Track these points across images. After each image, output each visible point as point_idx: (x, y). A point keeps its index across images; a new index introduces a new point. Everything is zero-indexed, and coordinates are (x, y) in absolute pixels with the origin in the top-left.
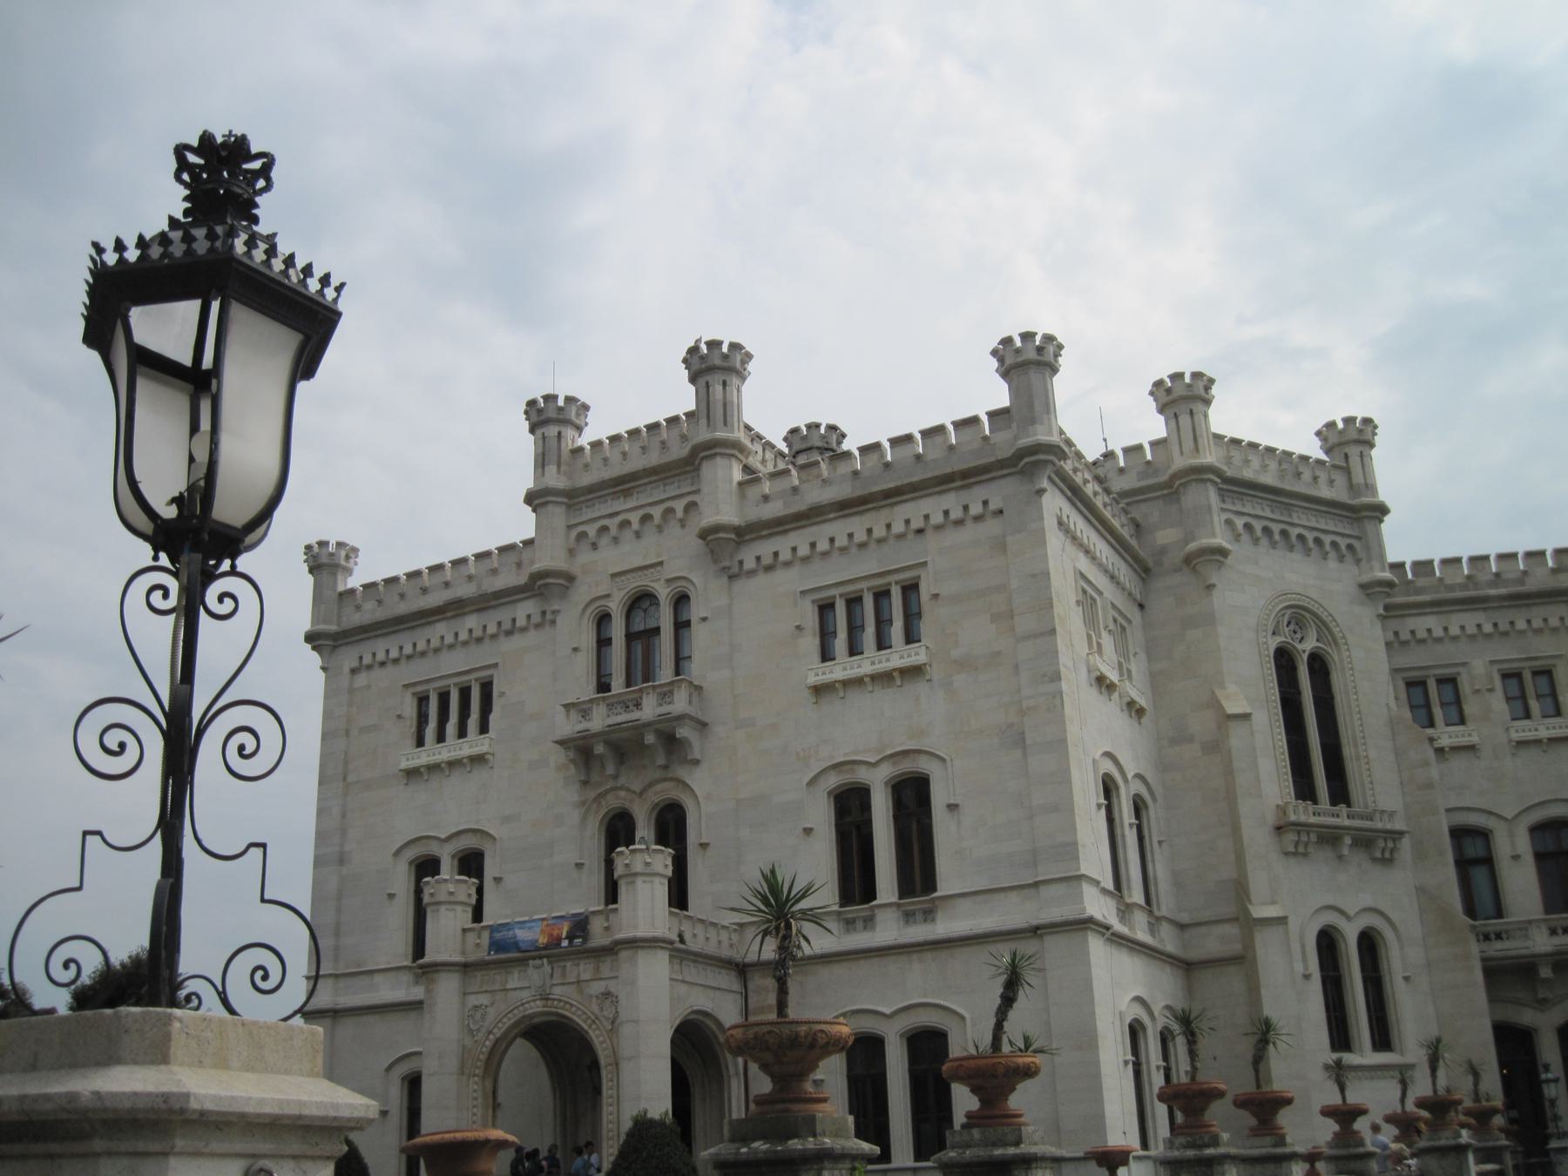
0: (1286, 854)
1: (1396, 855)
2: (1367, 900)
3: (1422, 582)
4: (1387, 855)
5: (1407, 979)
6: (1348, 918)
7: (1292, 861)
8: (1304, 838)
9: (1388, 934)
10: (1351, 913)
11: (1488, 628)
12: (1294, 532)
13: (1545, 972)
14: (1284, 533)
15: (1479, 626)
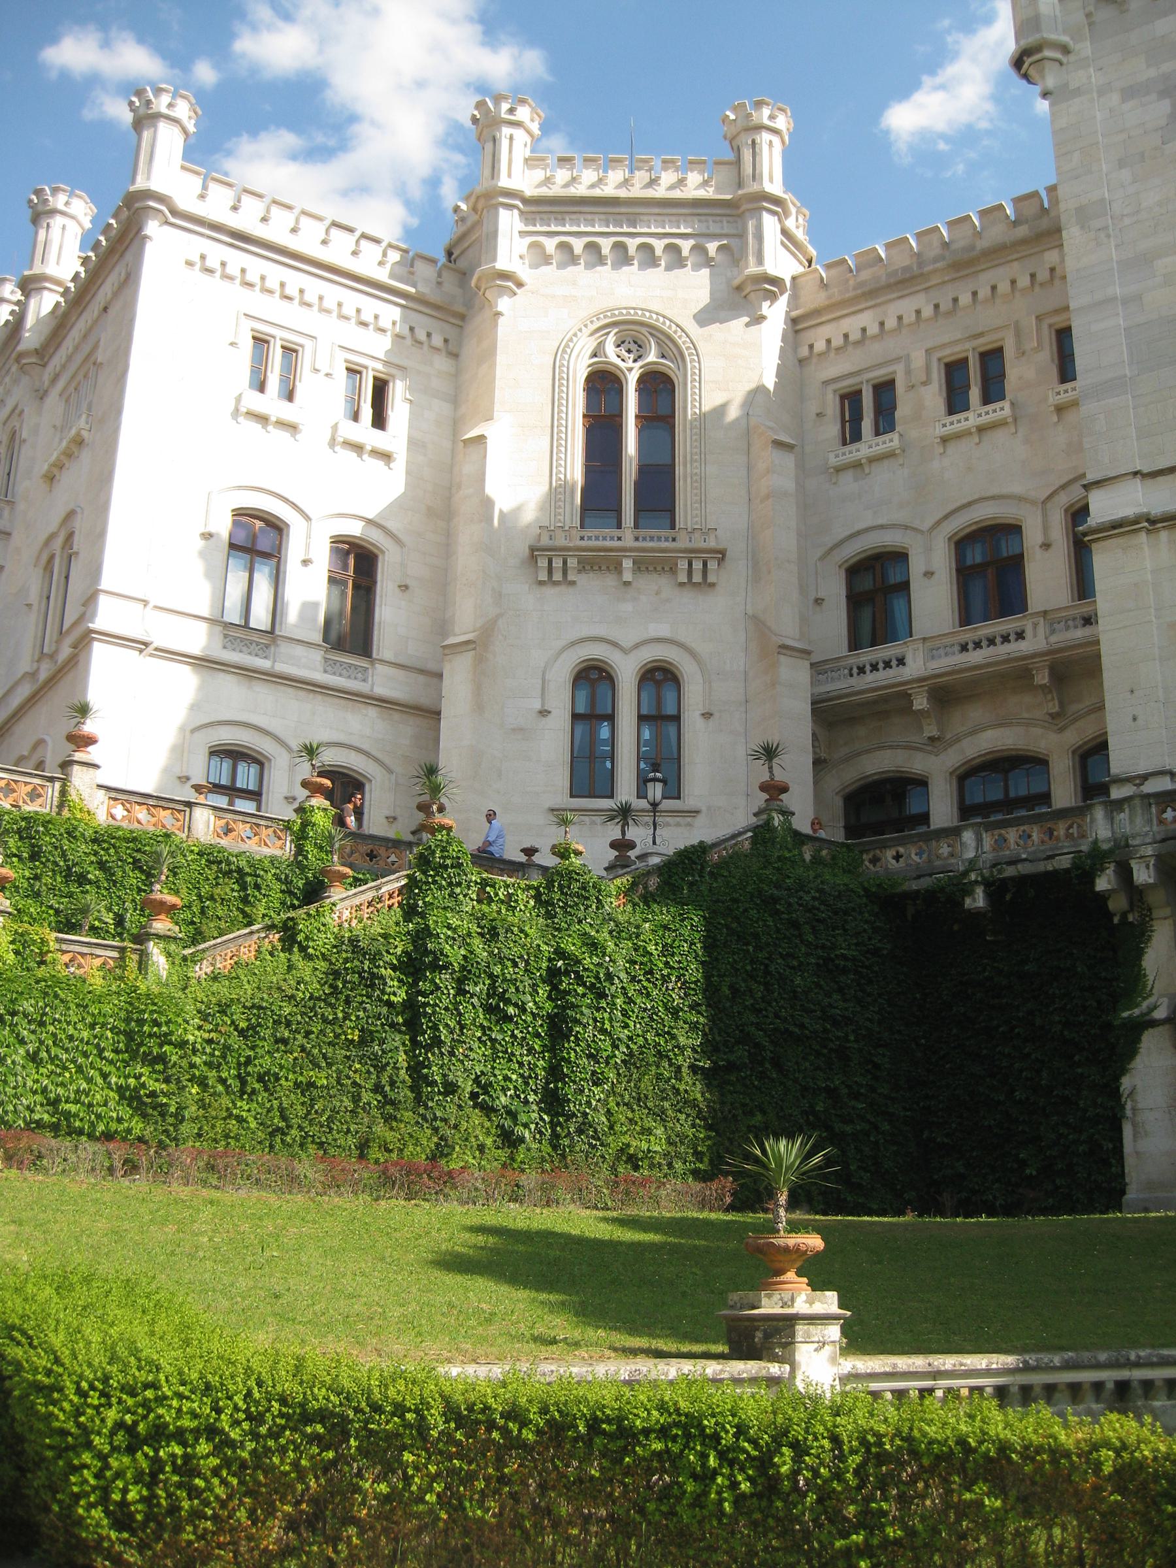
0: (541, 583)
1: (711, 578)
2: (663, 630)
3: (865, 275)
4: (697, 578)
5: (707, 715)
6: (625, 651)
7: (550, 591)
8: (557, 563)
9: (688, 669)
10: (626, 643)
11: (927, 312)
12: (632, 244)
13: (921, 703)
14: (620, 247)
15: (918, 312)
